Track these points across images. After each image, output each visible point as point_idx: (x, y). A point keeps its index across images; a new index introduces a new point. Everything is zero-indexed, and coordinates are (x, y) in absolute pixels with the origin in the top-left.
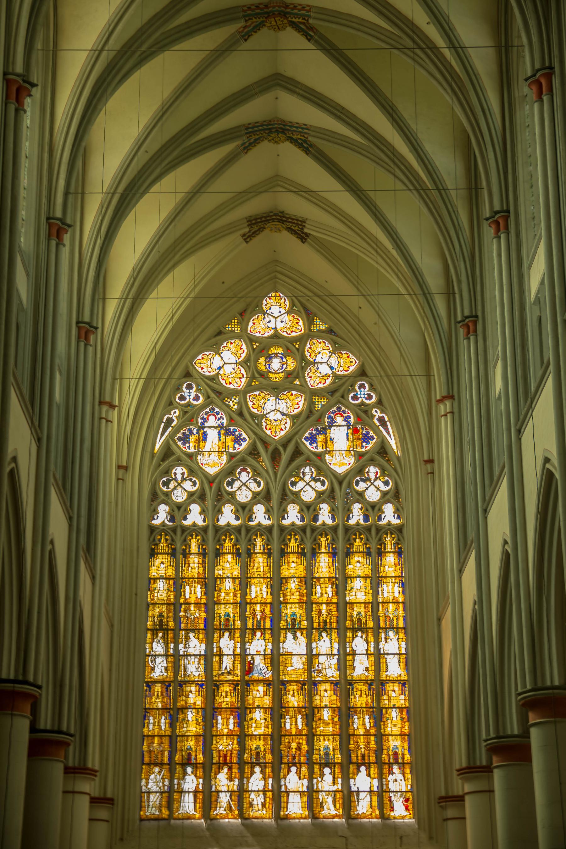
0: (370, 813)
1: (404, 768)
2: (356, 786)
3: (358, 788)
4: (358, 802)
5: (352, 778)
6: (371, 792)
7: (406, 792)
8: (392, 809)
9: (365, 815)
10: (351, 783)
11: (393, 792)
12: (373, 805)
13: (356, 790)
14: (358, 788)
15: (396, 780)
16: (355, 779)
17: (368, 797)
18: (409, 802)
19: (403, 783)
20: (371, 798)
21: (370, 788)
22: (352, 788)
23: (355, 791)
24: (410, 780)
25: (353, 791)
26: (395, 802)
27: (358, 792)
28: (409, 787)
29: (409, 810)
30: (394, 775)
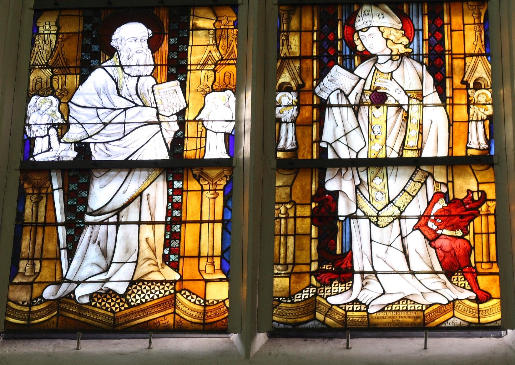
0: (159, 292)
1: (437, 30)
2: (75, 133)
3: (82, 148)
4: (75, 227)
5: (46, 90)
6: (178, 166)
7: (451, 163)
8: (339, 268)
9: (115, 305)
10: (33, 118)
11: (355, 163)
12: (189, 244)
13: (71, 154)
14: (82, 148)
15: (379, 98)
16: (65, 97)
17: (158, 193)
18: (479, 224)
19: (435, 118)
20: (174, 206)
21: (177, 144)
22: (40, 145)
23: (59, 165)
24: (484, 96)
25: (48, 167)
26: (360, 231)
27: (82, 170)
28: (477, 139)
29: (471, 274)
30: (363, 70)
